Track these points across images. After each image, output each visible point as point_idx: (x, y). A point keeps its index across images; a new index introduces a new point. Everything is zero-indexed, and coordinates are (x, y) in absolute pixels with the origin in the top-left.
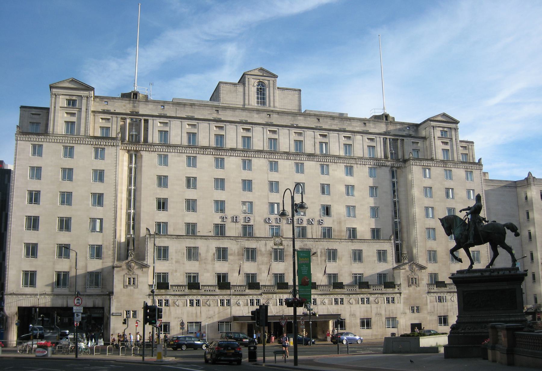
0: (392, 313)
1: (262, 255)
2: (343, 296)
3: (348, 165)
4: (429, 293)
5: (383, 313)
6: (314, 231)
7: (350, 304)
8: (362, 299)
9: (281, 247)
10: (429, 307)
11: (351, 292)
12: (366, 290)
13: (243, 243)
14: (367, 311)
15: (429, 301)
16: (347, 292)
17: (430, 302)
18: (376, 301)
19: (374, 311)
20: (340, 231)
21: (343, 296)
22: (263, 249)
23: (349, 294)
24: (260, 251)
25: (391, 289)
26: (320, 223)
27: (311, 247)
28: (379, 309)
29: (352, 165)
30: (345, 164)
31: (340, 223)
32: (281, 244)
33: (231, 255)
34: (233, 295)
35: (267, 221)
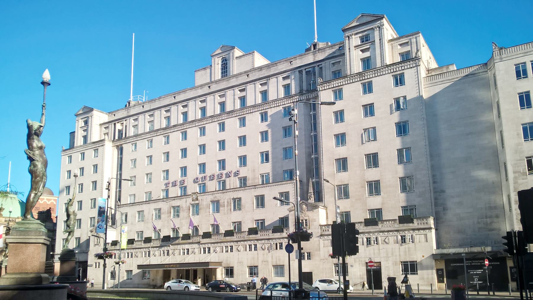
0: (279, 260)
1: (183, 211)
2: (232, 244)
3: (263, 111)
4: (321, 235)
5: (270, 259)
6: (232, 183)
7: (239, 251)
8: (250, 246)
9: (197, 202)
10: (322, 252)
11: (239, 239)
12: (254, 236)
13: (171, 203)
14: (253, 258)
15: (322, 245)
16: (235, 240)
17: (324, 247)
18: (263, 247)
19: (260, 259)
20: (254, 179)
21: (232, 243)
22: (184, 206)
23: (237, 241)
24: (182, 207)
25: (279, 234)
26: (236, 174)
27: (219, 199)
28: (265, 256)
29: (266, 110)
30: (260, 112)
31: (254, 171)
32: (197, 199)
33: (163, 213)
34: (152, 247)
35: (195, 181)
